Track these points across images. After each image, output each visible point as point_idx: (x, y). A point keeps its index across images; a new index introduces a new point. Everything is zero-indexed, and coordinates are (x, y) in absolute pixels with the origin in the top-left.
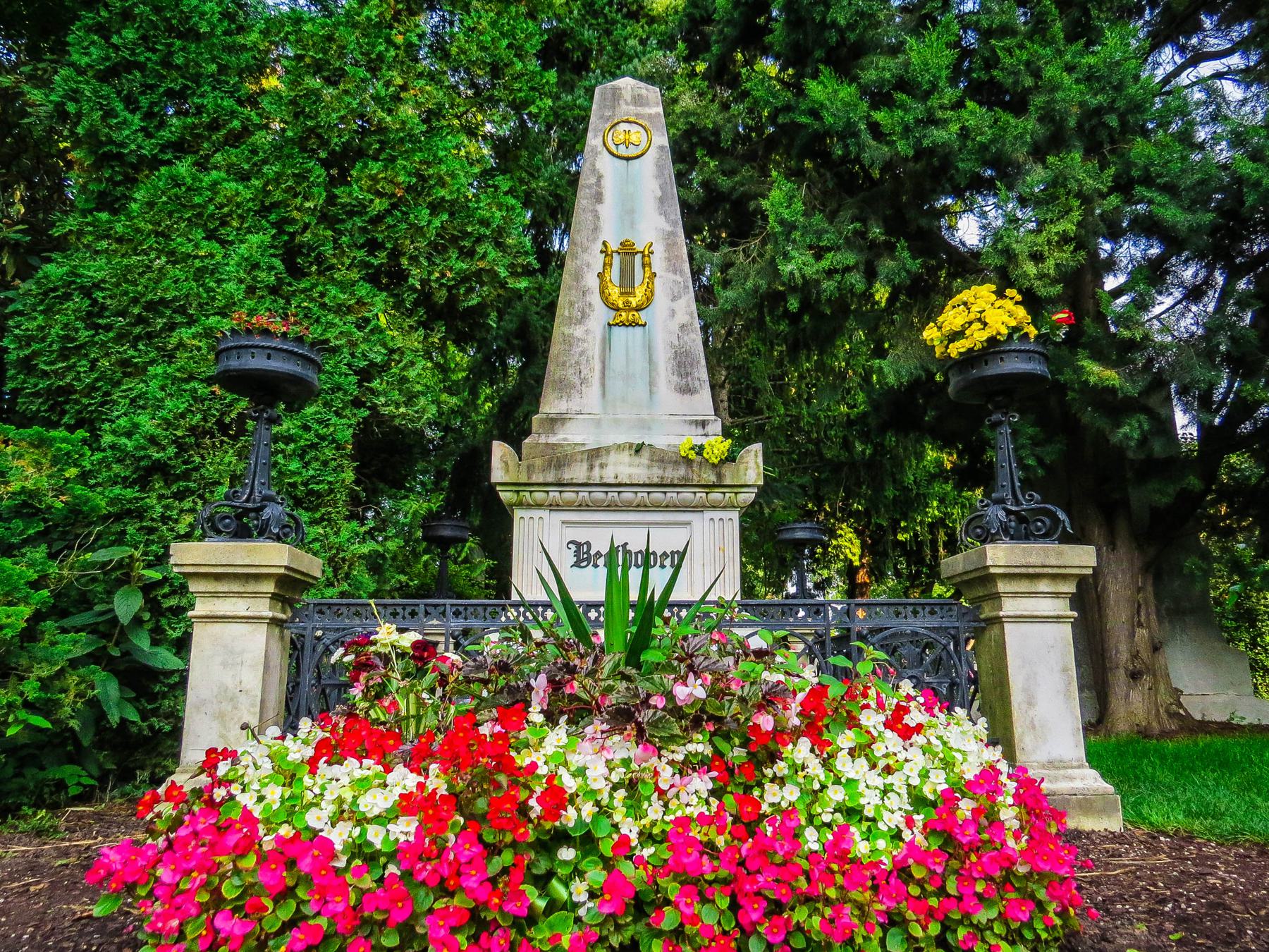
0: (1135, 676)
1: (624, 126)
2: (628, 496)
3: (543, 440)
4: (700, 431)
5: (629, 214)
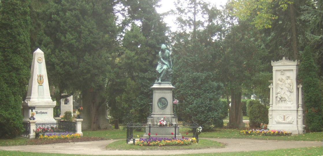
0: (94, 123)
1: (39, 58)
5: (40, 71)
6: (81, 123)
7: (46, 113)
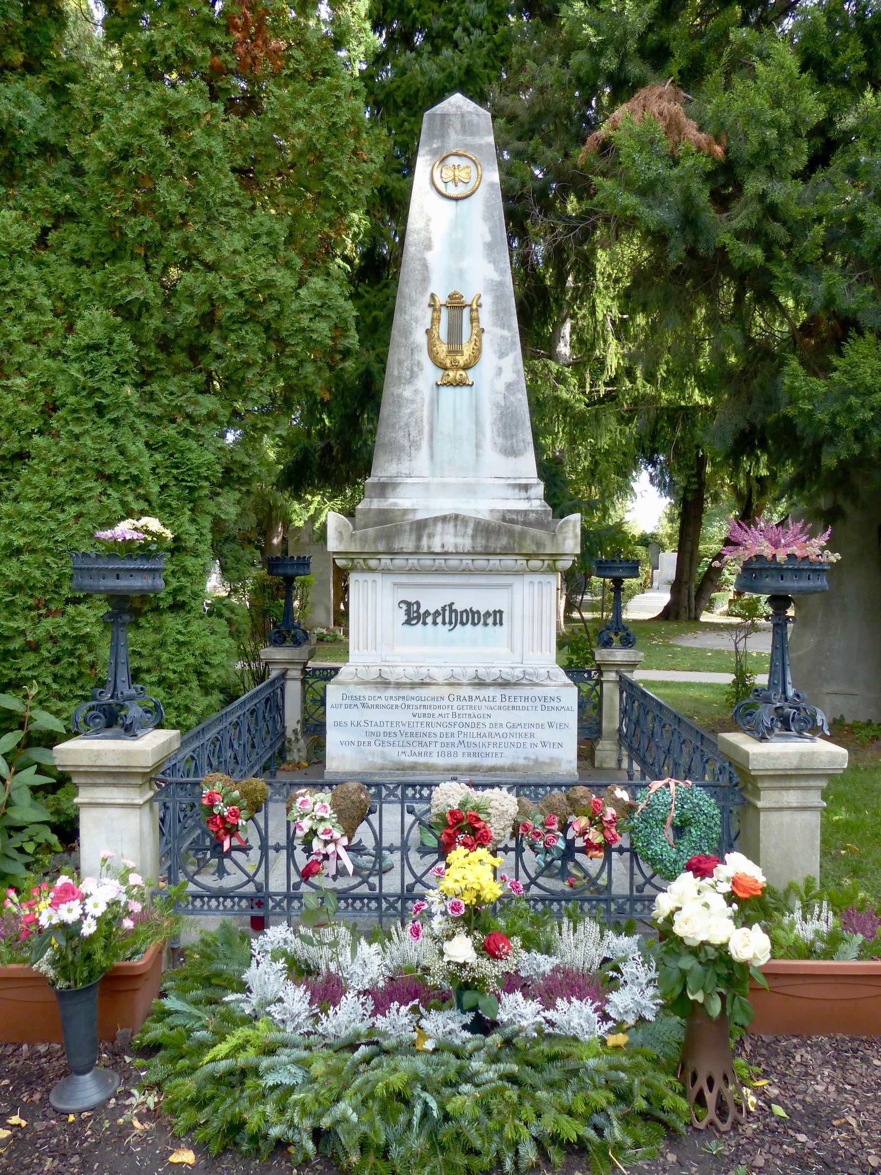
1: (453, 160)
2: (454, 562)
3: (376, 504)
4: (523, 494)
6: (815, 799)
7: (497, 617)
